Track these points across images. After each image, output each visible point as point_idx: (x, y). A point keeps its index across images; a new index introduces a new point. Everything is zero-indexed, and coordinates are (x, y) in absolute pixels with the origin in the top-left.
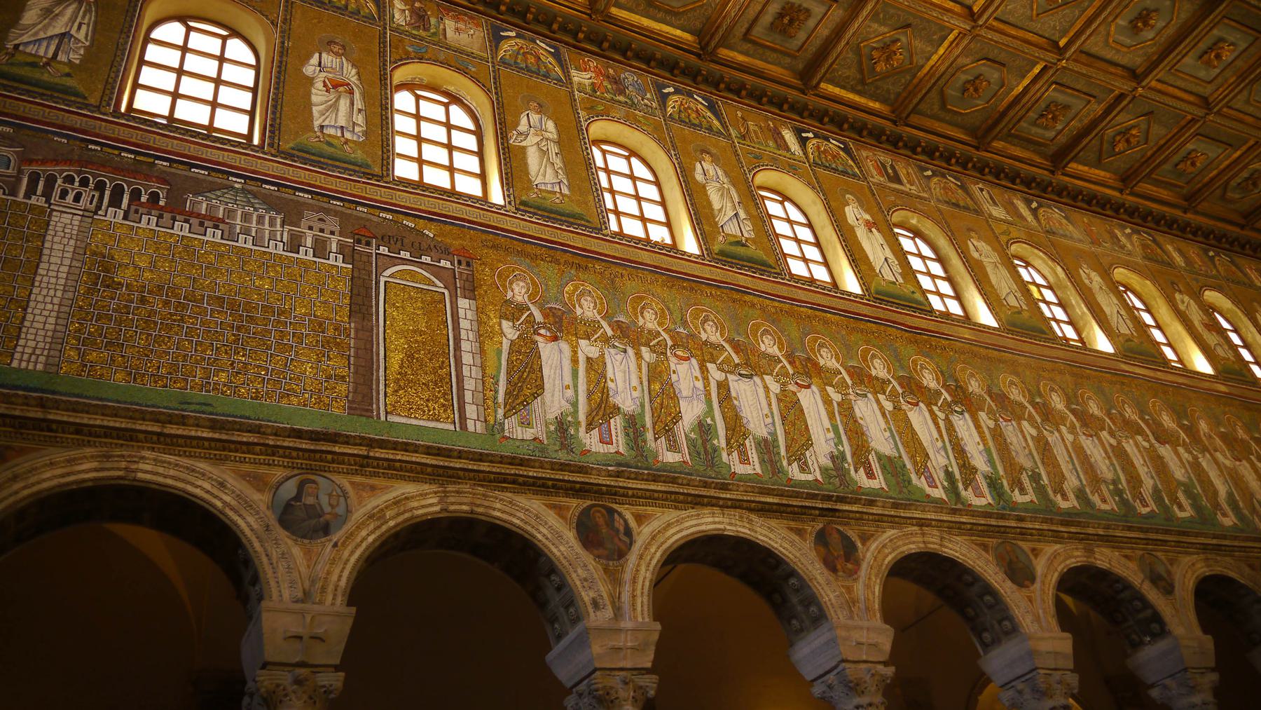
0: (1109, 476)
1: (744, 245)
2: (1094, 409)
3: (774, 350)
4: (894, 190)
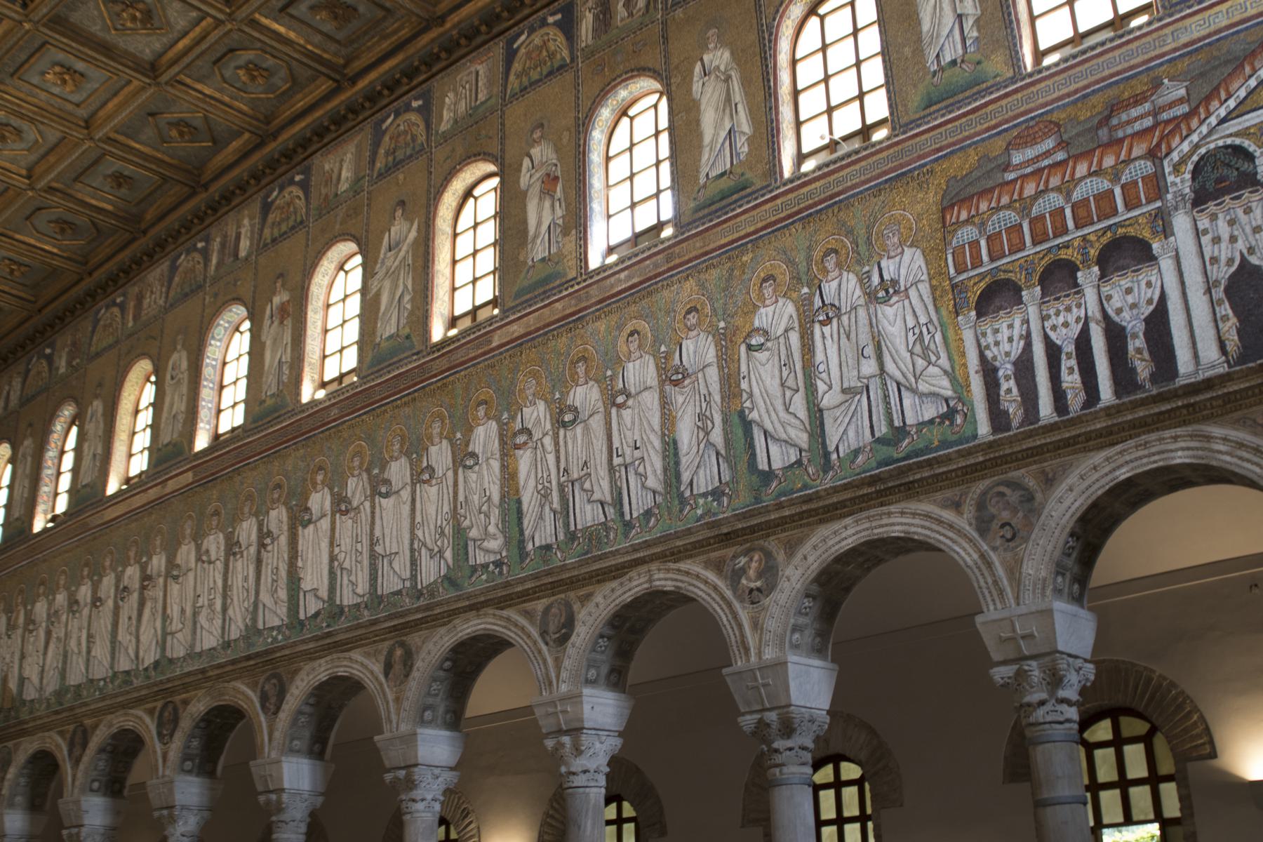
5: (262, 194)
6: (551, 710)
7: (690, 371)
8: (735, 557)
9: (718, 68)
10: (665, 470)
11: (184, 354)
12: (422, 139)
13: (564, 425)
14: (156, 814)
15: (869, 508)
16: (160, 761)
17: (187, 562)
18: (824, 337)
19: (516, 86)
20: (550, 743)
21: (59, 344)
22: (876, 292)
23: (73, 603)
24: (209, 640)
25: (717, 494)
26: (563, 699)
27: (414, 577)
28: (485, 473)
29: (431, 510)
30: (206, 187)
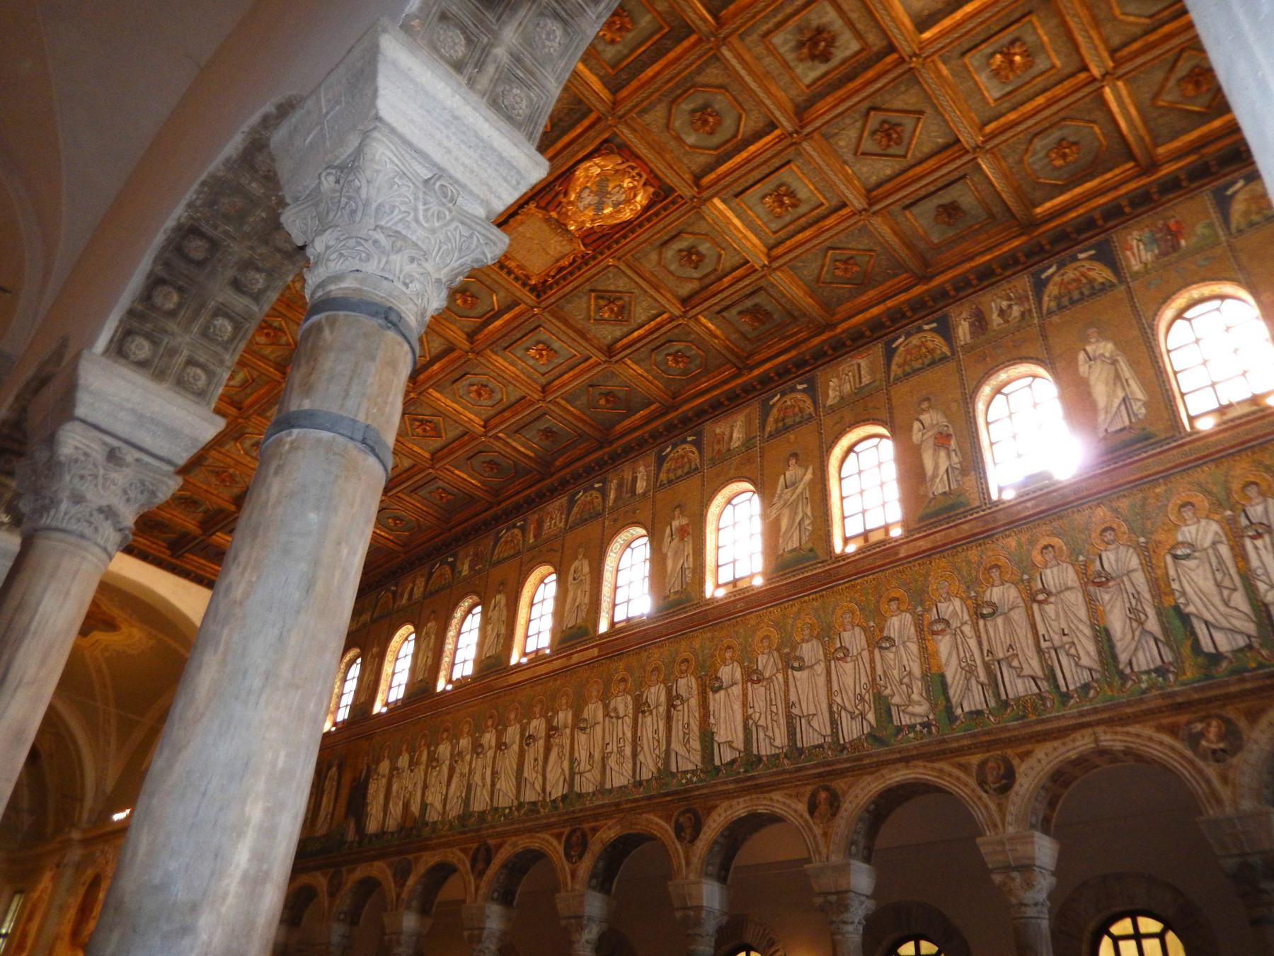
5: (656, 449)
6: (999, 848)
7: (1114, 575)
9: (1103, 355)
10: (1100, 653)
11: (586, 563)
13: (984, 617)
14: (563, 923)
16: (569, 877)
17: (595, 716)
18: (1256, 548)
19: (900, 372)
20: (997, 878)
21: (461, 554)
25: (1161, 671)
26: (1012, 839)
27: (835, 734)
28: (903, 653)
29: (849, 682)
30: (611, 443)
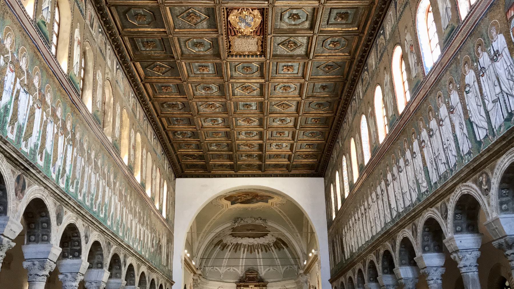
0: (92, 192)
1: (45, 25)
2: (99, 163)
3: (36, 84)
4: (90, 31)
8: (479, 177)
12: (385, 44)
15: (509, 149)
20: (452, 257)
22: (493, 57)
23: (355, 220)
24: (379, 229)
25: (469, 153)
